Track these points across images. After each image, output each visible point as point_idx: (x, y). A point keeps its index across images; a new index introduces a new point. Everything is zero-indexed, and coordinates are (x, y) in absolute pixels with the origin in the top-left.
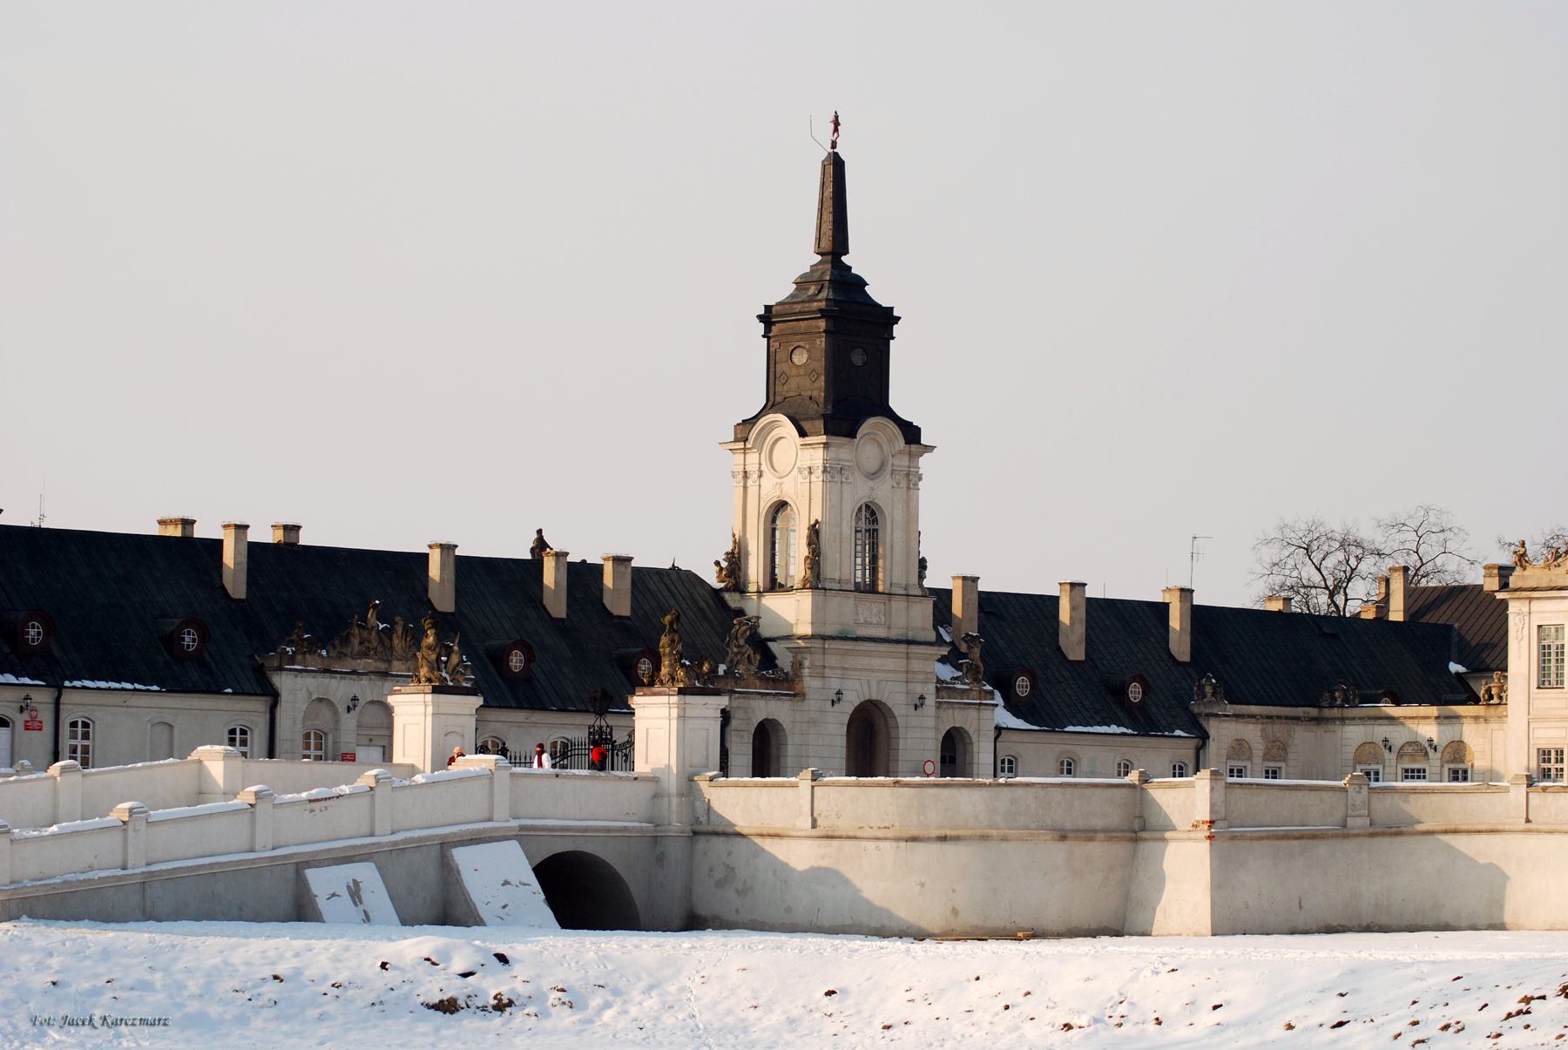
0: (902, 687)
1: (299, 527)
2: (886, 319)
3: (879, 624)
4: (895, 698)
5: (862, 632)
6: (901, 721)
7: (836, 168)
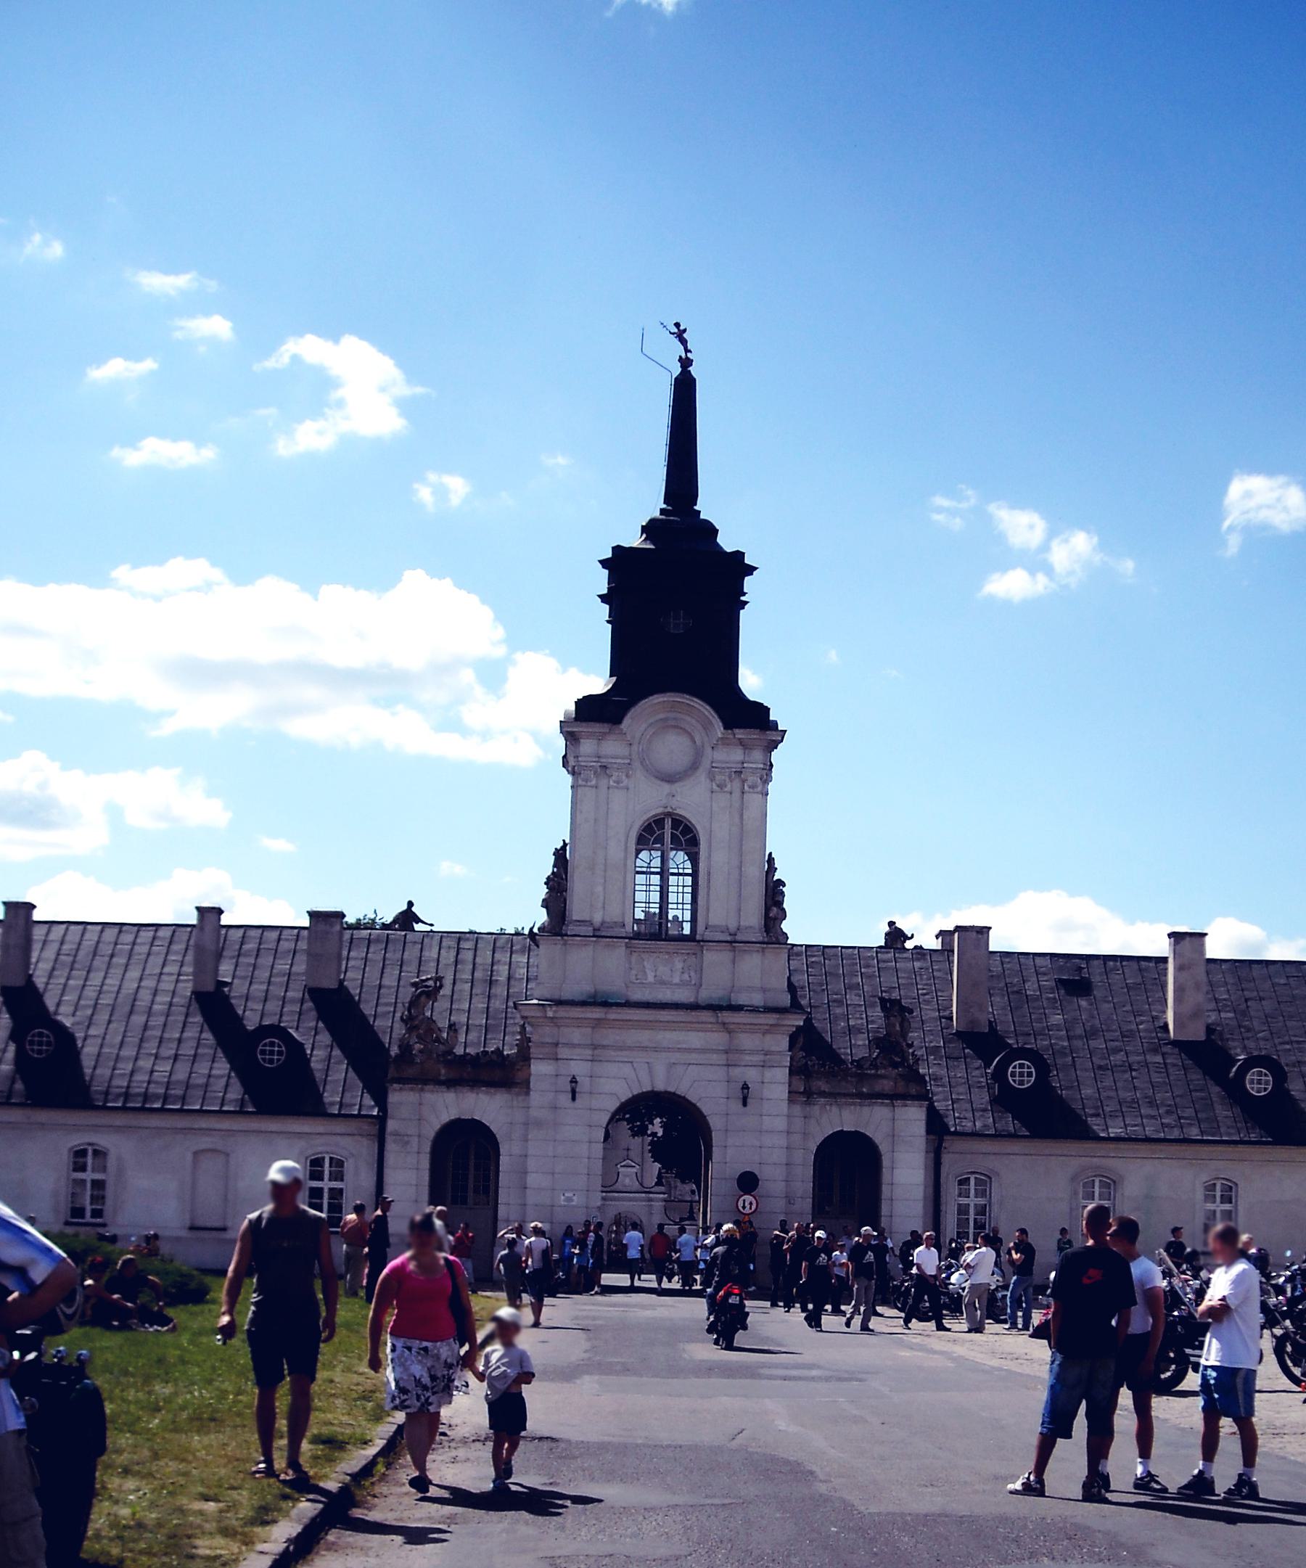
0: (720, 1073)
1: (34, 907)
2: (737, 567)
3: (683, 984)
4: (704, 1087)
5: (637, 995)
6: (715, 1122)
7: (684, 390)
